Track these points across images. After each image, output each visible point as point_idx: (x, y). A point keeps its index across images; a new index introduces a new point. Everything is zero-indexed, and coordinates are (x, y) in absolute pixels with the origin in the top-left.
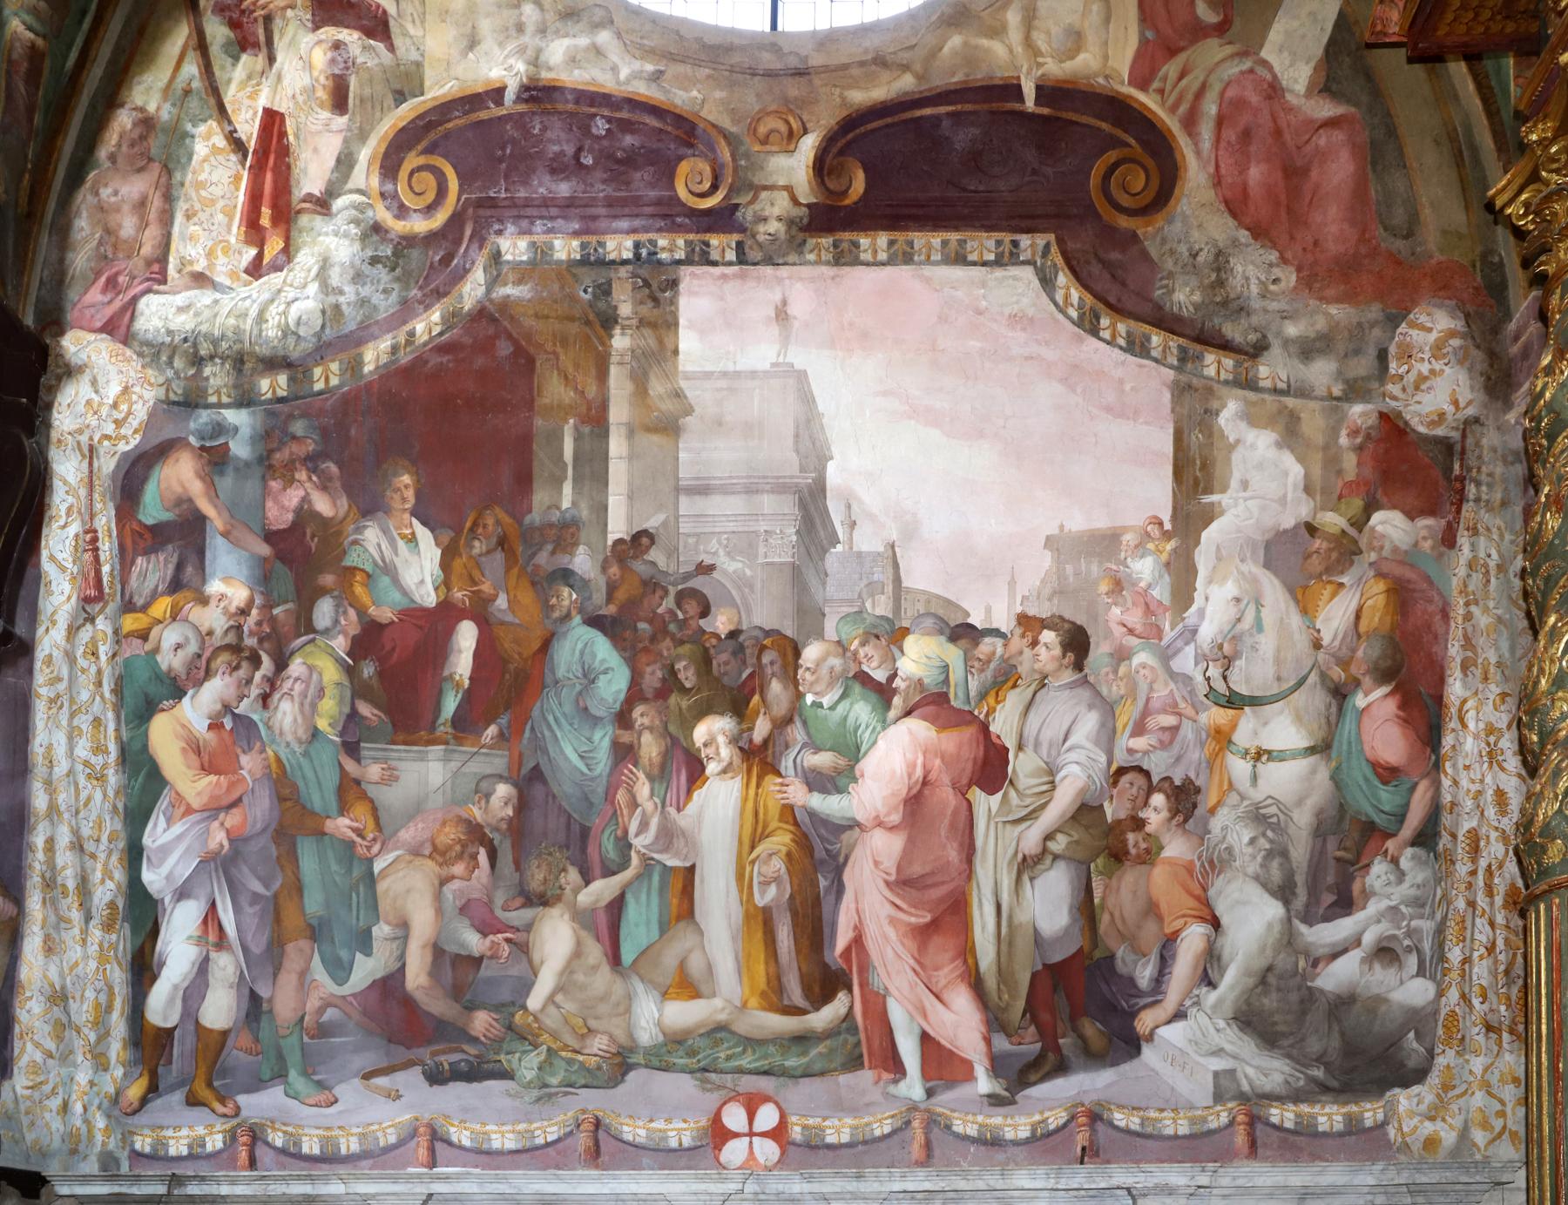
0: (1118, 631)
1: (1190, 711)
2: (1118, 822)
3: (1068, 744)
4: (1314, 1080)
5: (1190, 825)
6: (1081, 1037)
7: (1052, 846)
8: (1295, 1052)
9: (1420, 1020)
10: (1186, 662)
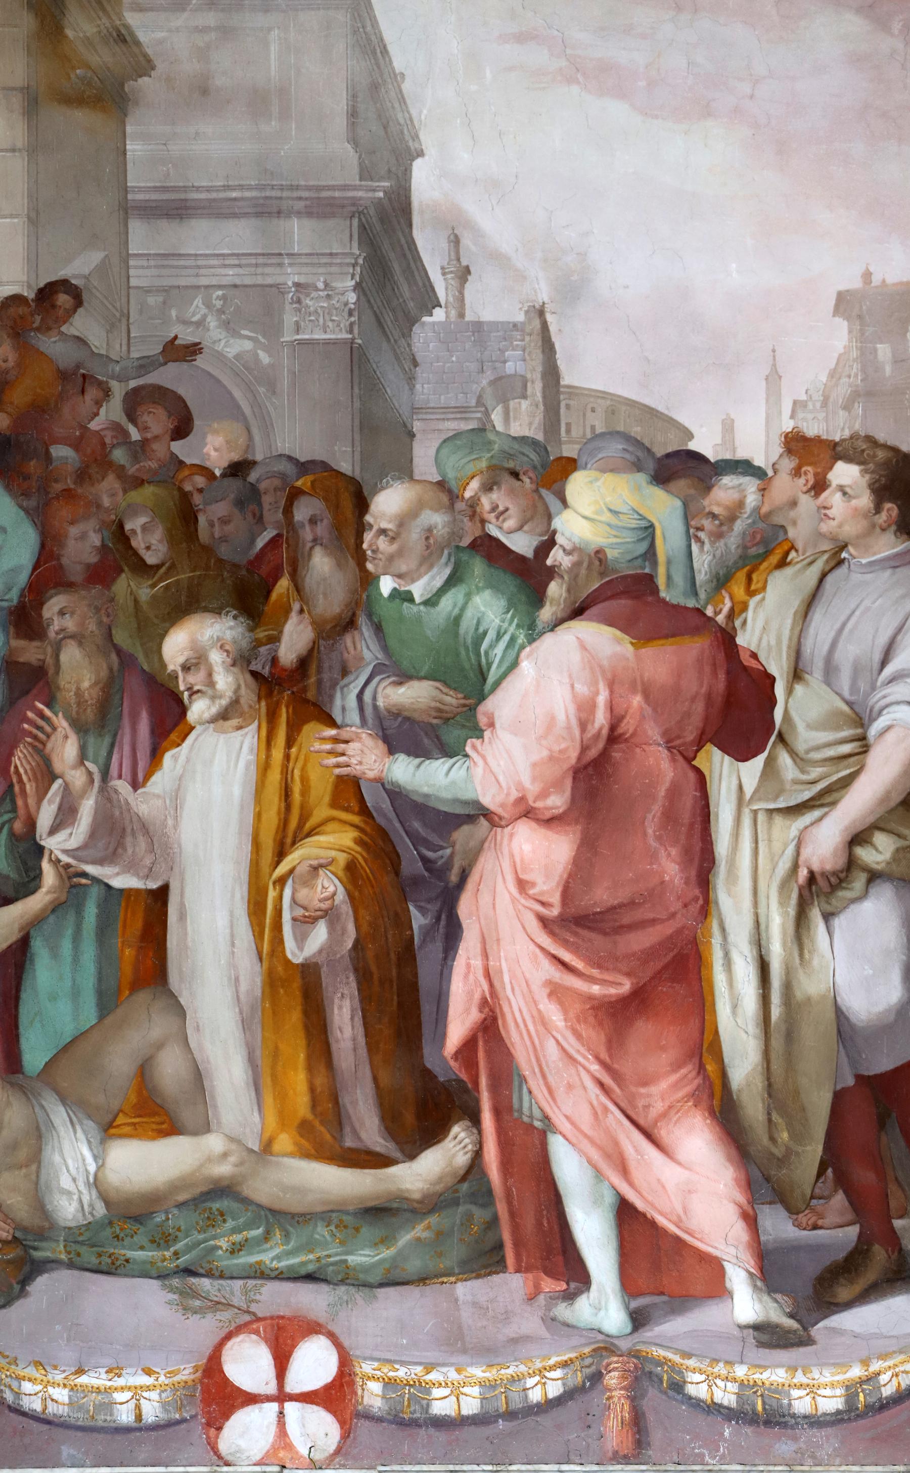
3: (889, 670)
7: (865, 854)
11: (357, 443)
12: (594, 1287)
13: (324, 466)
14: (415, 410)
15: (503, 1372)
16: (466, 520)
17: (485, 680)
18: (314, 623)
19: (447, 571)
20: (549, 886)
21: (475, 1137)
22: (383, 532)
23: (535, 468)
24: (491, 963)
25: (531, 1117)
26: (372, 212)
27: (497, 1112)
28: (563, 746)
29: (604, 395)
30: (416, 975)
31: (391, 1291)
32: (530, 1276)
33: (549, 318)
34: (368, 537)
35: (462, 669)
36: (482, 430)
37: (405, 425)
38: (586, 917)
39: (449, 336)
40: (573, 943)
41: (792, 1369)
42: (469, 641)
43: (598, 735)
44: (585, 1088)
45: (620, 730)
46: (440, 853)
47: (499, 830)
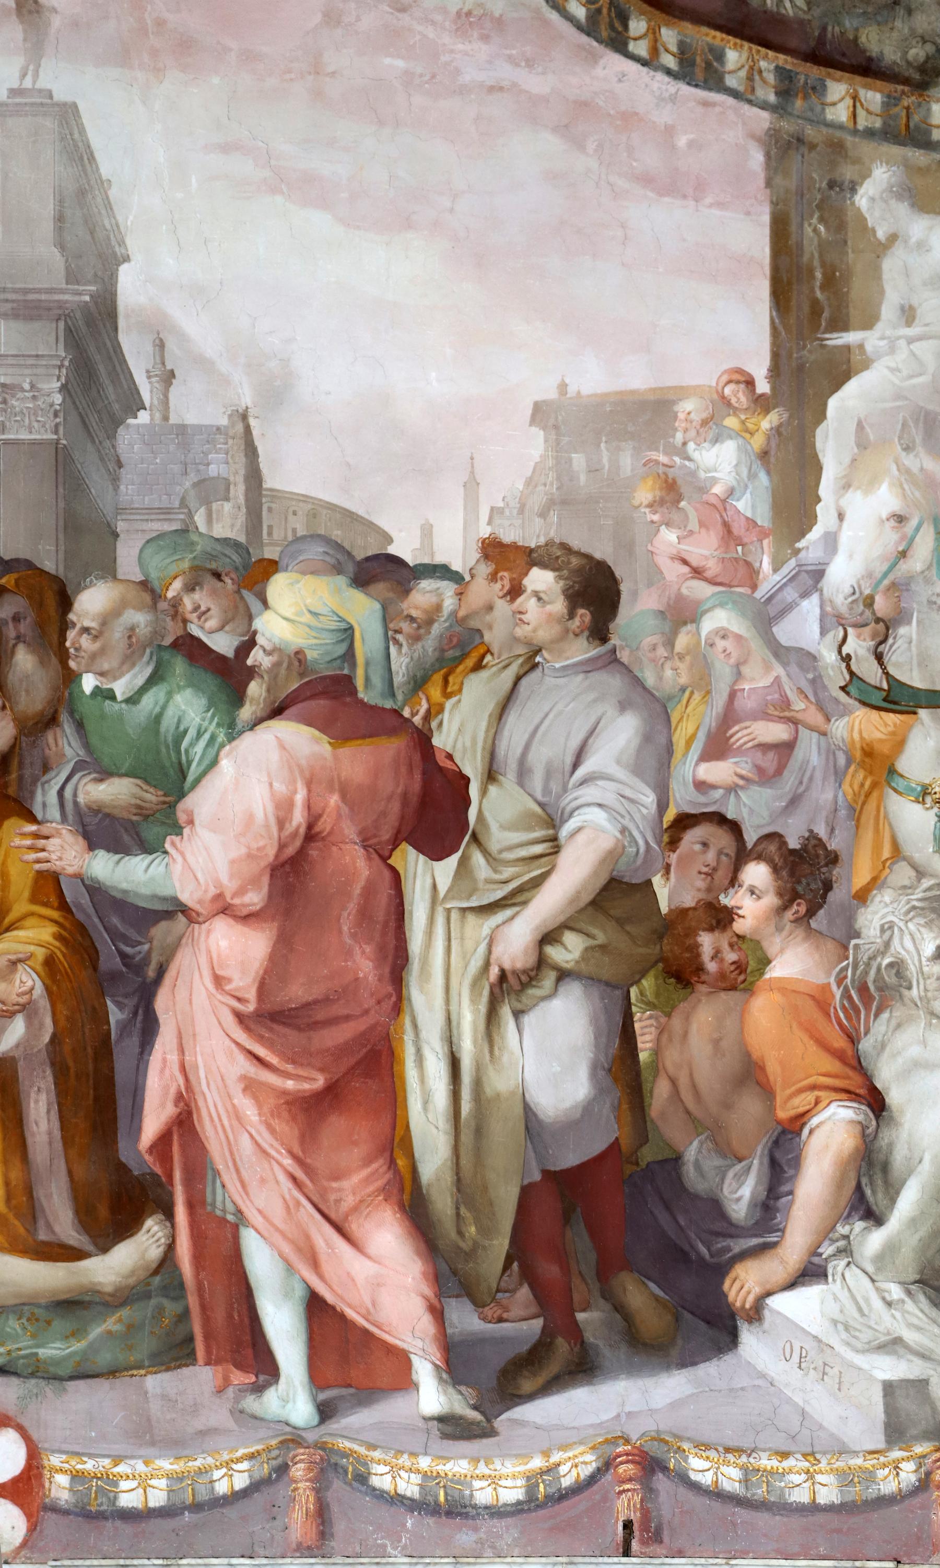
0: (673, 572)
1: (814, 717)
2: (681, 913)
3: (580, 772)
5: (819, 921)
6: (619, 1308)
7: (555, 953)
10: (803, 626)
11: (61, 542)
12: (282, 1380)
13: (29, 564)
14: (119, 510)
15: (190, 1464)
16: (168, 619)
17: (185, 778)
18: (15, 720)
19: (149, 670)
20: (245, 982)
21: (168, 1230)
22: (86, 630)
23: (237, 569)
24: (187, 1058)
25: (224, 1211)
26: (78, 315)
27: (191, 1206)
28: (261, 843)
29: (305, 499)
30: (112, 1069)
31: (81, 1384)
32: (220, 1368)
33: (252, 422)
34: (71, 635)
35: (163, 767)
36: (184, 531)
37: (109, 525)
38: (281, 1012)
39: (152, 438)
40: (268, 1039)
41: (475, 1460)
42: (170, 739)
43: (295, 834)
44: (277, 1182)
45: (317, 829)
46: (138, 948)
47: (196, 926)
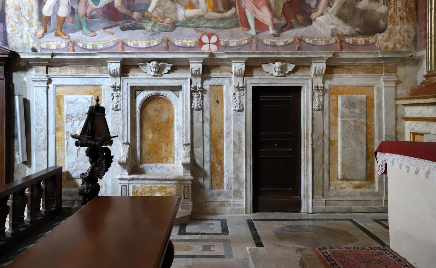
4: (357, 32)
6: (297, 19)
8: (352, 24)
9: (384, 16)
